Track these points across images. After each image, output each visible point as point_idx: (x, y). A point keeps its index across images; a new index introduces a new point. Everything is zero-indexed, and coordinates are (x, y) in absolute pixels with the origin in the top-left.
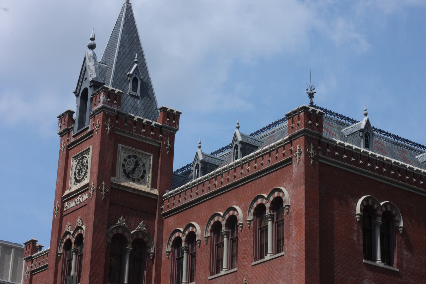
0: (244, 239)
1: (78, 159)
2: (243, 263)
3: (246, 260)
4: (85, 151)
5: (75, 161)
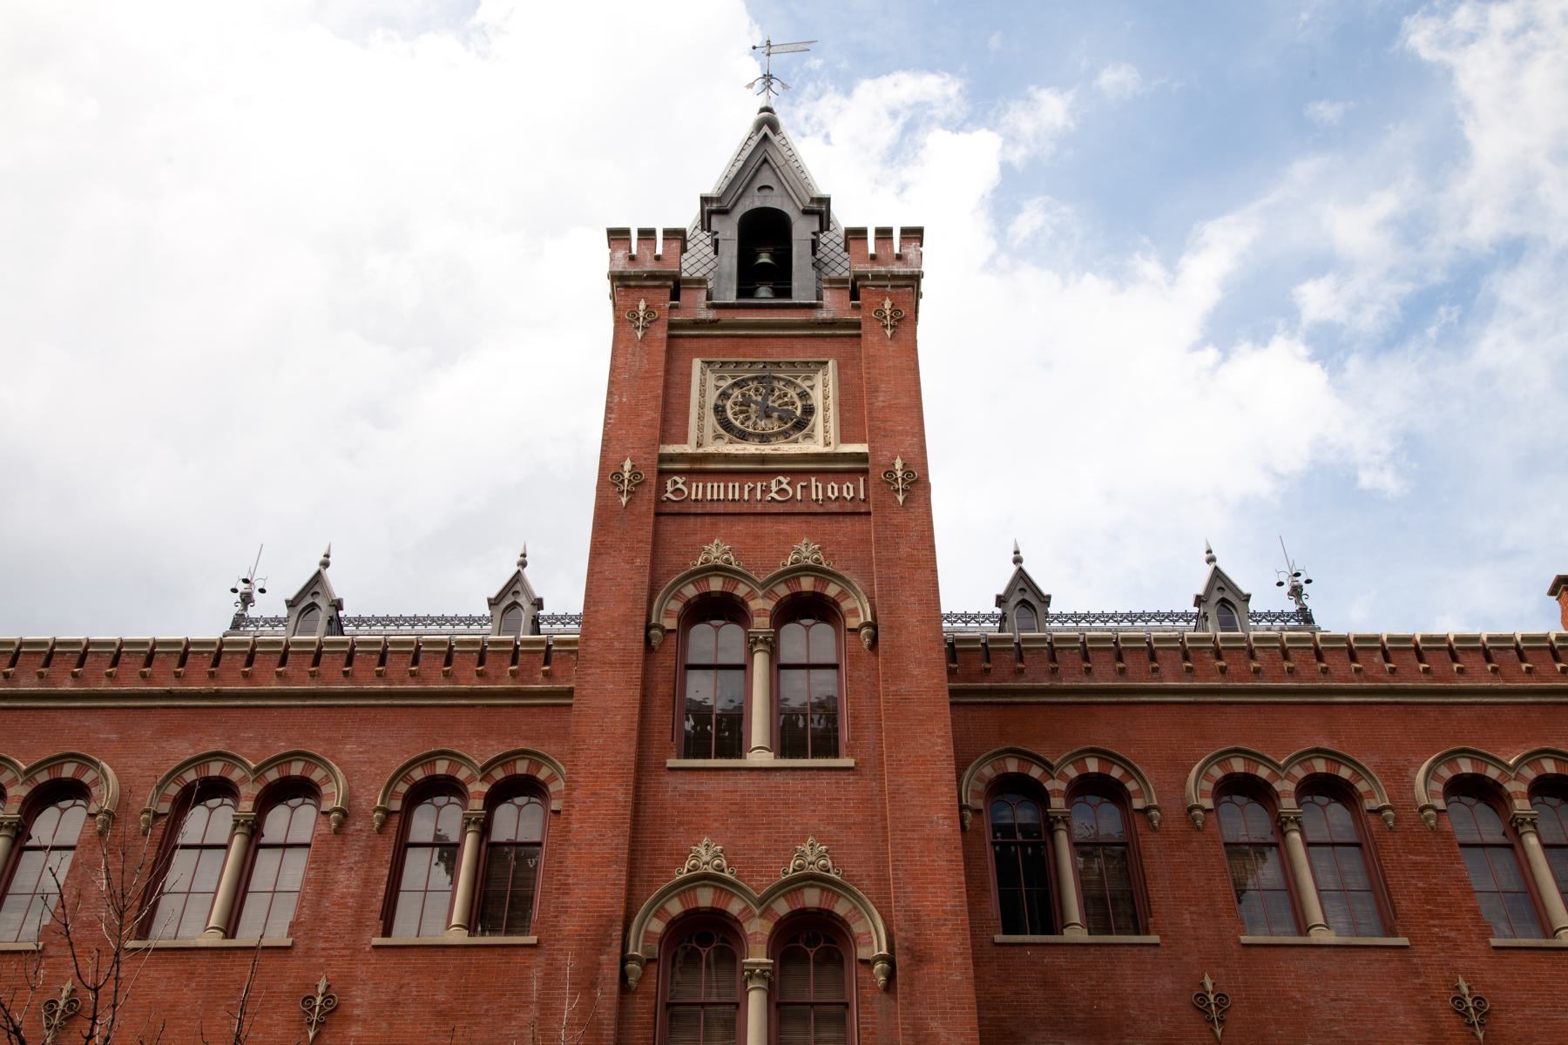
2: (1437, 930)
3: (1446, 922)
4: (793, 364)
5: (711, 379)
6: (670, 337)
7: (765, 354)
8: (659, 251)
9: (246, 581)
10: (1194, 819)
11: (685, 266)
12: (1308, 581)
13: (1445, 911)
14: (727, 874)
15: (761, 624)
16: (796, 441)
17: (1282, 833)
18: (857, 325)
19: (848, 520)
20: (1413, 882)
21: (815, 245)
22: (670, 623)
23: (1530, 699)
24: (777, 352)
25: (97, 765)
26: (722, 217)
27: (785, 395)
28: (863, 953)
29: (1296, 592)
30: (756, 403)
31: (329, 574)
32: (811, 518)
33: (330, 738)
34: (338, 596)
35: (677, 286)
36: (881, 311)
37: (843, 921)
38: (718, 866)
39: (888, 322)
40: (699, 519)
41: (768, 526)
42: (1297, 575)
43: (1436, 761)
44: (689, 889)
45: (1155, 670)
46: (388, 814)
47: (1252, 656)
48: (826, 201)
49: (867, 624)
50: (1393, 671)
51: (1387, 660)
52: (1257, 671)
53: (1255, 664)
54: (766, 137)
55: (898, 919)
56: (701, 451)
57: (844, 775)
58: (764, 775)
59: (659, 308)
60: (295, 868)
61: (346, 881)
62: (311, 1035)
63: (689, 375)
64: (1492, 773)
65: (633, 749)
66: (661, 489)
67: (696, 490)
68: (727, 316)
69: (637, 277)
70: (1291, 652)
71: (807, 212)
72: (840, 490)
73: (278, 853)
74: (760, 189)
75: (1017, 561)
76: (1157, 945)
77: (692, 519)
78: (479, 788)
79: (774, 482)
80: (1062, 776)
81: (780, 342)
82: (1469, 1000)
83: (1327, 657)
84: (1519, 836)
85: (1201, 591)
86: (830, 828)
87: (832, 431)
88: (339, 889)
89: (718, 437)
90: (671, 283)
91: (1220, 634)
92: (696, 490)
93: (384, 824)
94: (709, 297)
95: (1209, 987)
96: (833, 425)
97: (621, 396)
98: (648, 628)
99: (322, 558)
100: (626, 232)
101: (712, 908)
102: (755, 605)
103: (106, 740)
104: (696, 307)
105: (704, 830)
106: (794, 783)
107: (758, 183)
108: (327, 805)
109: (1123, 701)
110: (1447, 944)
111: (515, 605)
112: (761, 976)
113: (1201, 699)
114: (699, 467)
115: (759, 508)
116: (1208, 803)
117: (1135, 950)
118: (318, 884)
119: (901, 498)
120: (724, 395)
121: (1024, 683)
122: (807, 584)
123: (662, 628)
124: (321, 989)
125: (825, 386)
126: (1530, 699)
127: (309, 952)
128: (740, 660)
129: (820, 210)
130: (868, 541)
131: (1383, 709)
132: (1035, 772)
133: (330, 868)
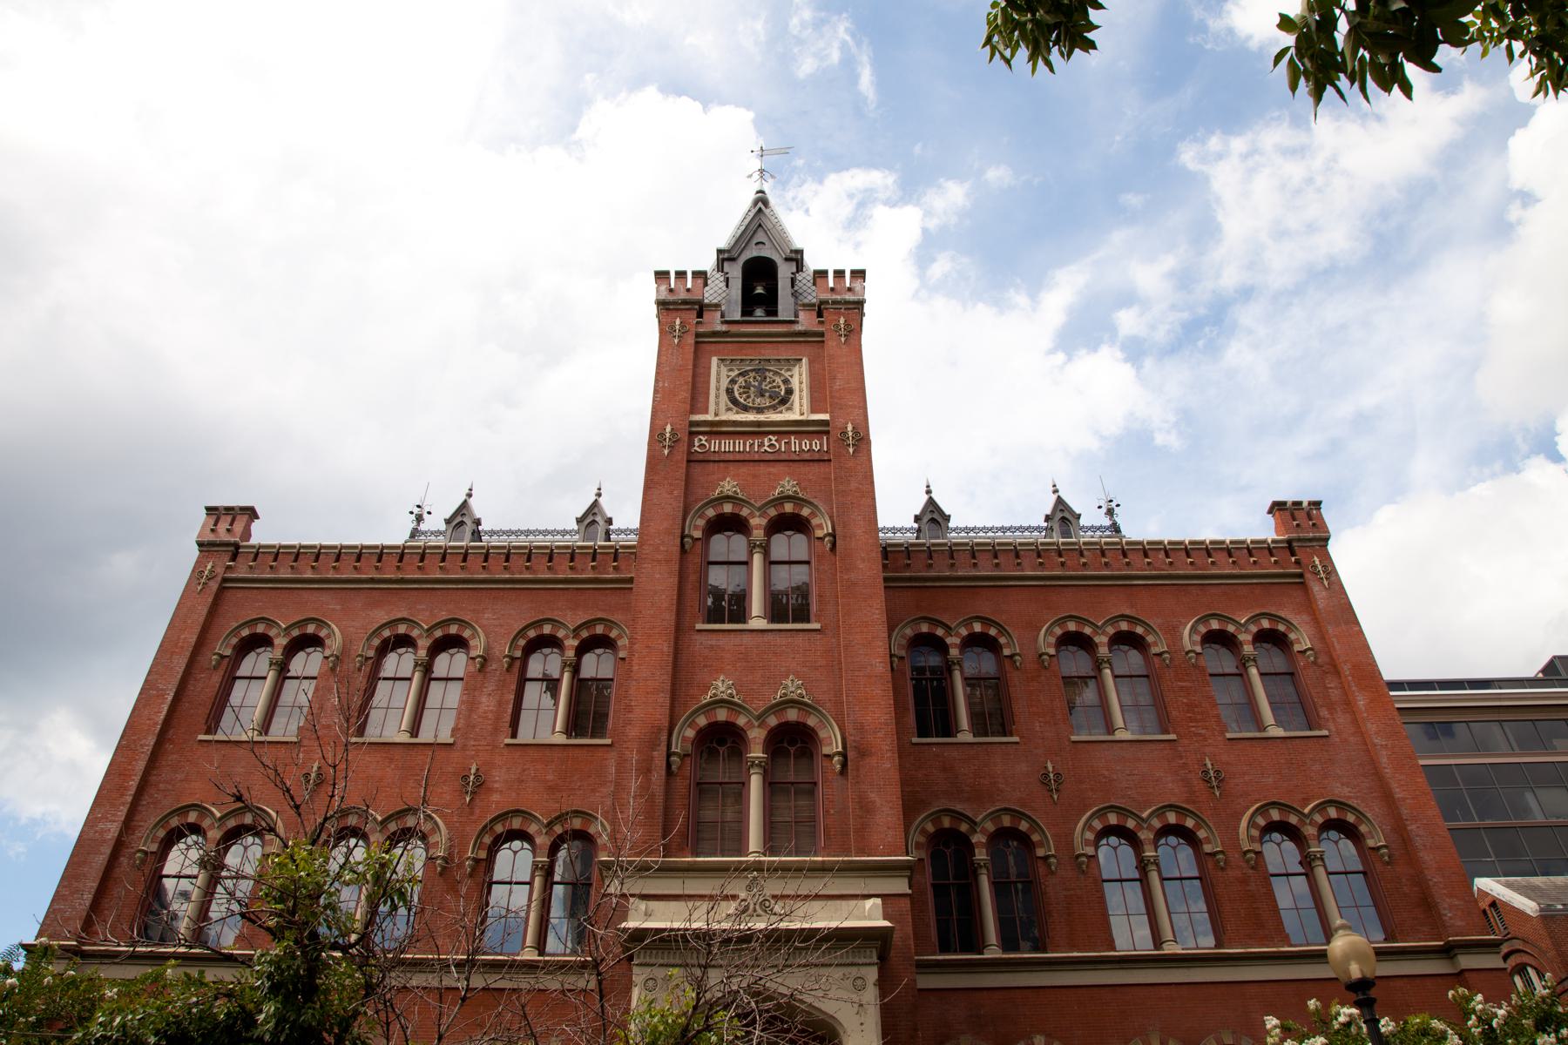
0: (1179, 683)
1: (739, 370)
3: (1200, 724)
4: (779, 360)
5: (724, 370)
6: (697, 343)
7: (760, 354)
8: (689, 285)
9: (419, 506)
10: (1043, 661)
11: (706, 295)
12: (1118, 505)
13: (1199, 717)
14: (736, 700)
15: (758, 534)
16: (781, 412)
17: (1099, 669)
18: (822, 334)
19: (816, 464)
20: (1181, 699)
21: (793, 281)
22: (698, 534)
23: (1255, 581)
24: (769, 352)
25: (329, 626)
26: (731, 263)
27: (774, 381)
28: (826, 750)
29: (1110, 512)
30: (754, 386)
31: (472, 501)
32: (791, 464)
33: (474, 610)
34: (478, 517)
35: (701, 308)
36: (838, 325)
37: (813, 730)
38: (731, 694)
39: (842, 332)
40: (716, 464)
41: (763, 469)
42: (1111, 501)
43: (1196, 622)
44: (711, 709)
45: (1019, 564)
46: (513, 659)
47: (1082, 554)
48: (801, 252)
49: (829, 534)
50: (1171, 563)
51: (1167, 556)
52: (1085, 564)
53: (1084, 560)
54: (760, 209)
55: (849, 728)
56: (717, 419)
57: (813, 634)
58: (760, 634)
59: (689, 324)
60: (454, 693)
61: (487, 703)
62: (468, 799)
63: (710, 368)
64: (1231, 628)
65: (674, 617)
66: (691, 444)
67: (714, 445)
68: (734, 329)
69: (674, 303)
70: (1106, 552)
71: (787, 259)
72: (811, 445)
73: (442, 684)
74: (757, 244)
75: (929, 492)
76: (1017, 743)
77: (711, 464)
78: (572, 643)
79: (766, 440)
80: (958, 635)
81: (770, 345)
82: (1212, 772)
83: (1130, 555)
84: (1246, 669)
85: (1049, 512)
86: (805, 669)
87: (805, 405)
88: (483, 708)
89: (729, 409)
90: (697, 307)
91: (1061, 540)
92: (714, 445)
93: (510, 665)
94: (722, 316)
95: (1050, 769)
96: (805, 402)
97: (664, 382)
98: (683, 537)
99: (467, 491)
100: (667, 273)
101: (726, 722)
102: (754, 521)
103: (333, 610)
104: (714, 322)
105: (721, 671)
106: (780, 640)
107: (755, 241)
108: (473, 653)
109: (998, 585)
110: (1201, 738)
111: (594, 522)
112: (759, 765)
113: (1048, 583)
114: (716, 430)
115: (757, 457)
116: (1052, 651)
117: (1003, 747)
118: (469, 704)
119: (851, 450)
120: (733, 381)
121: (933, 574)
122: (789, 508)
123: (692, 537)
124: (473, 771)
125: (800, 375)
126: (1255, 581)
127: (464, 748)
128: (743, 558)
129: (796, 258)
130: (830, 479)
131: (1165, 588)
132: (940, 632)
133: (476, 693)
